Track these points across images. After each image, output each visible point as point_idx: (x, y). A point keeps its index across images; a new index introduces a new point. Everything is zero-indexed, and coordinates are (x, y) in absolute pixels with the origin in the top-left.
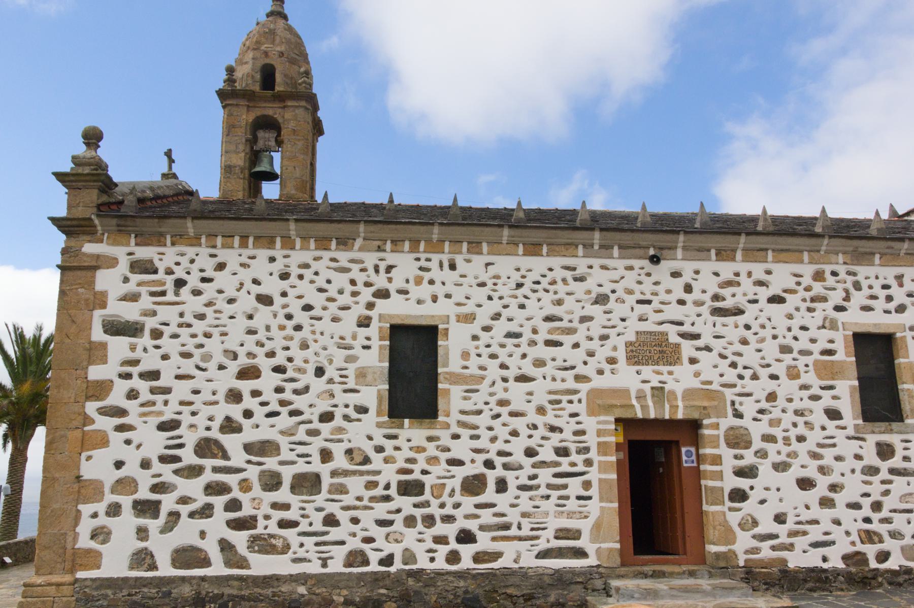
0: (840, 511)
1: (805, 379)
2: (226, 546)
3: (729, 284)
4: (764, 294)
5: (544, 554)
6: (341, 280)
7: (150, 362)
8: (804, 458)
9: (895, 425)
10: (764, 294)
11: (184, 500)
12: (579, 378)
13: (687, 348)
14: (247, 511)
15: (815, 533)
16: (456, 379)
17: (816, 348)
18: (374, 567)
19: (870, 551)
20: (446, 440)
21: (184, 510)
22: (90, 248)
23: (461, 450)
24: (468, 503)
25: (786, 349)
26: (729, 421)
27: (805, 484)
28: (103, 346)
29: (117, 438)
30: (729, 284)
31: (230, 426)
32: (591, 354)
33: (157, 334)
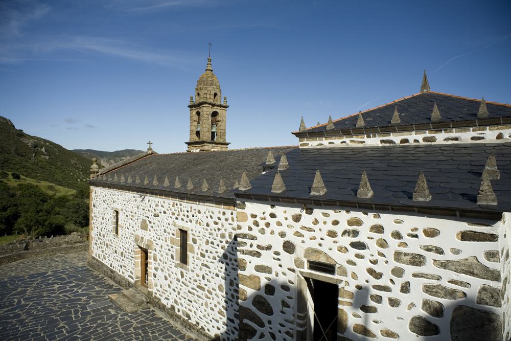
18: (112, 268)
19: (176, 307)
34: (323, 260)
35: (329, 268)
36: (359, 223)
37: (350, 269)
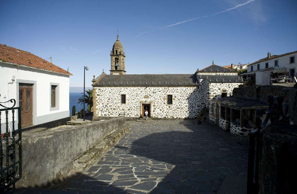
0: (164, 113)
1: (162, 100)
2: (108, 114)
3: (155, 90)
4: (158, 91)
5: (135, 116)
6: (117, 90)
7: (101, 98)
8: (161, 108)
9: (171, 104)
10: (158, 91)
11: (104, 110)
12: (139, 100)
13: (150, 97)
14: (109, 111)
15: (161, 115)
16: (127, 100)
17: (163, 97)
19: (167, 117)
20: (126, 105)
21: (105, 111)
22: (95, 88)
23: (128, 106)
24: (128, 111)
25: (160, 97)
26: (153, 104)
27: (161, 110)
28: (97, 97)
29: (99, 105)
30: (155, 90)
31: (108, 104)
32: (140, 97)
33: (101, 96)
34: (225, 90)
35: (226, 91)
36: (229, 84)
37: (229, 90)
